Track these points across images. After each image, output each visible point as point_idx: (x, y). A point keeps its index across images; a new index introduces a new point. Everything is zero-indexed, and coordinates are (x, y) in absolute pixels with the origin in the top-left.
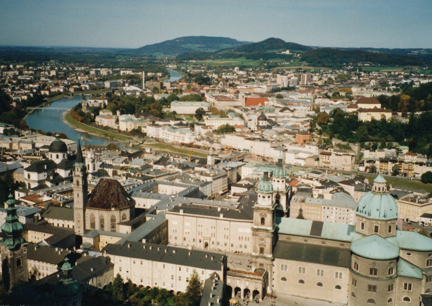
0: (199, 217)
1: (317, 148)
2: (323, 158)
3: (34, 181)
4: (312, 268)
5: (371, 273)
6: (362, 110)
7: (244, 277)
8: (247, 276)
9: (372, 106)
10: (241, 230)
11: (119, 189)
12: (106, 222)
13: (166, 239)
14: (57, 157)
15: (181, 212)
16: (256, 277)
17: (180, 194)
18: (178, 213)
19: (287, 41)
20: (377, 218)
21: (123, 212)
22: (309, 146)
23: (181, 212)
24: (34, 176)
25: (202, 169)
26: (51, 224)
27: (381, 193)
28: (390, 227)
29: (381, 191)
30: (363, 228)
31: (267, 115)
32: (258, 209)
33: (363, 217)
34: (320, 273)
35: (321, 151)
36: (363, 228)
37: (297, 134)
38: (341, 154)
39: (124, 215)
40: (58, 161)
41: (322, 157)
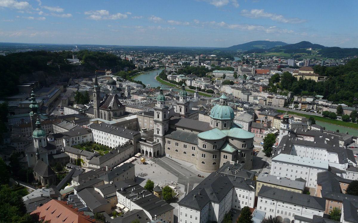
0: (151, 117)
2: (268, 100)
4: (182, 144)
5: (203, 147)
12: (106, 115)
15: (143, 114)
19: (313, 44)
22: (264, 93)
34: (185, 146)
37: (260, 87)
41: (268, 99)
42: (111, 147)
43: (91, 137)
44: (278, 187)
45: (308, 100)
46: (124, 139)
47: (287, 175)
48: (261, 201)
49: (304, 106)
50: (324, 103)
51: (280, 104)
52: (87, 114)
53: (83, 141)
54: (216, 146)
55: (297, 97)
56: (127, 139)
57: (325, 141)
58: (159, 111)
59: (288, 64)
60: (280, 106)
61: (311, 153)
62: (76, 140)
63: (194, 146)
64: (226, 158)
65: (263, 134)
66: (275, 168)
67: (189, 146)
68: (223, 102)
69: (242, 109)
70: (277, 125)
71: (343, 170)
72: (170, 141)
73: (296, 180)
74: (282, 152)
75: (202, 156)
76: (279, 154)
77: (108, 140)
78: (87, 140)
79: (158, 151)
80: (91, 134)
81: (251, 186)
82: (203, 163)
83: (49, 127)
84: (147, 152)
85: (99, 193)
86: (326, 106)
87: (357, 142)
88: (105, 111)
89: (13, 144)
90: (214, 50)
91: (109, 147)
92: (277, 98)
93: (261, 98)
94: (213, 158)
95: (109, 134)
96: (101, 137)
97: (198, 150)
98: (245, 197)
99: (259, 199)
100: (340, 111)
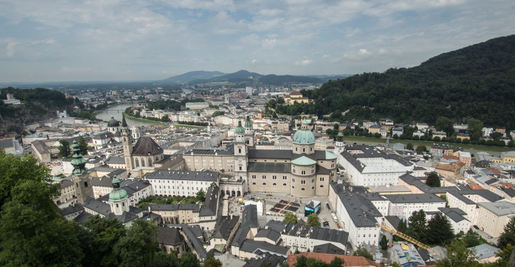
3: (100, 146)
5: (302, 174)
6: (292, 99)
7: (232, 184)
8: (233, 183)
9: (298, 96)
10: (228, 161)
15: (192, 154)
16: (238, 183)
17: (192, 146)
19: (251, 72)
20: (304, 144)
21: (155, 156)
23: (192, 154)
24: (99, 142)
25: (205, 133)
28: (311, 148)
29: (305, 128)
30: (296, 150)
31: (241, 107)
32: (237, 143)
33: (296, 144)
35: (272, 121)
36: (296, 150)
37: (258, 114)
42: (184, 197)
43: (150, 190)
46: (204, 182)
52: (110, 165)
53: (143, 196)
58: (241, 145)
59: (247, 92)
64: (323, 180)
67: (279, 176)
68: (306, 127)
75: (302, 183)
77: (178, 188)
82: (303, 189)
83: (72, 189)
84: (234, 192)
85: (266, 242)
86: (325, 125)
88: (142, 157)
93: (265, 125)
95: (180, 182)
96: (167, 187)
97: (293, 177)
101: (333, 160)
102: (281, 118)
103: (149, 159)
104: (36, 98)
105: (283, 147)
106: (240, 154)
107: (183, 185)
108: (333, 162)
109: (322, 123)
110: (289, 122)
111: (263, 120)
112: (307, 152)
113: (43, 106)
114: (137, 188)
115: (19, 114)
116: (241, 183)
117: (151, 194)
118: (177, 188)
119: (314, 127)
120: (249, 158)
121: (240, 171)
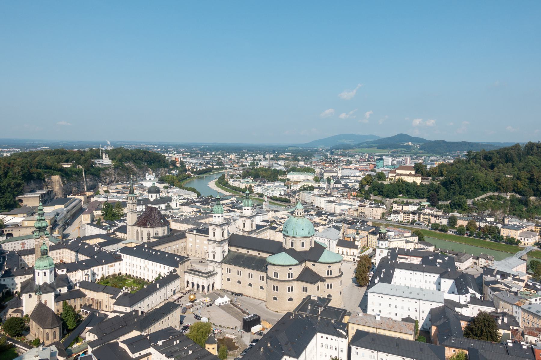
1: (358, 201)
4: (246, 272)
5: (275, 276)
6: (398, 175)
8: (198, 273)
9: (408, 172)
11: (156, 214)
13: (159, 244)
14: (152, 197)
15: (195, 232)
18: (192, 233)
19: (412, 136)
22: (353, 201)
26: (117, 236)
27: (298, 217)
28: (303, 244)
34: (251, 276)
38: (374, 206)
39: (157, 232)
40: (152, 200)
41: (359, 208)
44: (378, 330)
45: (410, 208)
46: (166, 267)
47: (390, 313)
48: (357, 353)
49: (406, 216)
50: (432, 212)
51: (375, 215)
52: (118, 234)
53: (108, 273)
54: (292, 274)
55: (396, 205)
56: (171, 267)
57: (437, 264)
60: (376, 217)
61: (420, 281)
62: (98, 271)
63: (264, 275)
64: (306, 291)
65: (355, 256)
66: (373, 303)
67: (257, 274)
69: (326, 222)
70: (373, 243)
71: (465, 303)
72: (230, 269)
73: (404, 320)
74: (381, 281)
75: (274, 290)
76: (377, 283)
78: (114, 271)
79: (213, 284)
80: (121, 262)
81: (341, 331)
83: (61, 253)
86: (436, 216)
87: (479, 263)
89: (4, 281)
90: (289, 147)
91: (146, 280)
92: (371, 207)
94: (289, 291)
95: (146, 261)
96: (135, 266)
98: (334, 348)
99: (353, 348)
100: (452, 221)
101: (329, 264)
102: (374, 200)
103: (149, 232)
104: (128, 159)
105: (321, 238)
106: (214, 239)
107: (148, 266)
108: (329, 267)
109: (431, 212)
110: (384, 207)
111: (351, 202)
112: (298, 248)
113: (134, 168)
114: (104, 261)
115: (105, 174)
116: (206, 276)
117: (121, 271)
118: (143, 268)
119: (419, 217)
120: (229, 246)
121: (214, 260)
